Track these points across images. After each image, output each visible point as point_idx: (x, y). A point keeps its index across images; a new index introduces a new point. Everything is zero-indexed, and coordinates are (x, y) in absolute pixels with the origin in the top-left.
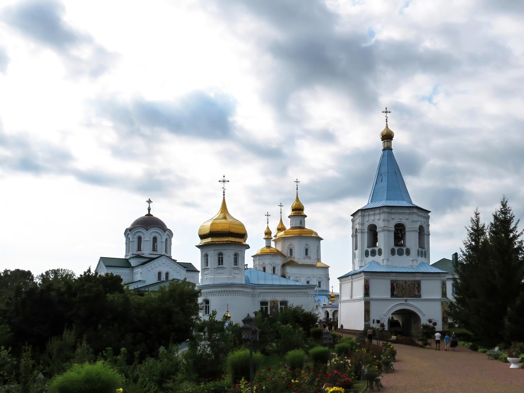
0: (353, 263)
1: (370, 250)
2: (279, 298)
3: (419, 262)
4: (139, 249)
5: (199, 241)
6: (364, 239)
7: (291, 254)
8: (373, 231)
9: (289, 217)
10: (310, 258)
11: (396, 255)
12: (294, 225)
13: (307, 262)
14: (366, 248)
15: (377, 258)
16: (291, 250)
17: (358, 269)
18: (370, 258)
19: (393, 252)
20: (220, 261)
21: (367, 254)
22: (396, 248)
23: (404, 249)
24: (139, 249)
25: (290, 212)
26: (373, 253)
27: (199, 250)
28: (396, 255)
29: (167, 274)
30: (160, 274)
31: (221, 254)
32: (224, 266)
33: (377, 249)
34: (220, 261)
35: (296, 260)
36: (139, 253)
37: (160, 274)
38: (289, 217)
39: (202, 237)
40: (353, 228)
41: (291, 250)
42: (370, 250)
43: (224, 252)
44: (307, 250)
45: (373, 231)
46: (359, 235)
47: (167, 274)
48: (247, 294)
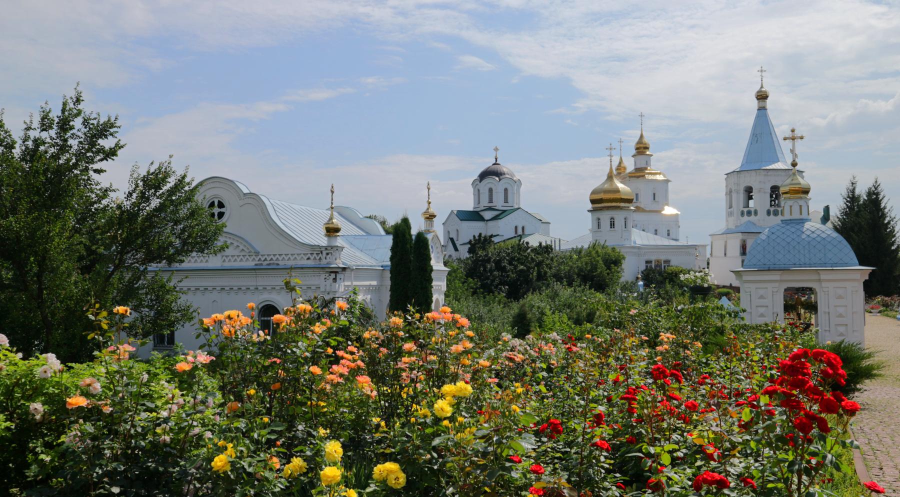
0: (727, 221)
1: (746, 210)
2: (663, 258)
4: (491, 201)
5: (590, 206)
8: (749, 191)
11: (772, 216)
12: (638, 166)
13: (654, 207)
15: (753, 218)
16: (637, 195)
17: (732, 227)
18: (746, 218)
19: (769, 213)
20: (612, 225)
21: (742, 214)
22: (772, 209)
23: (780, 209)
24: (491, 201)
25: (634, 152)
26: (749, 213)
27: (590, 214)
28: (772, 216)
29: (523, 228)
30: (516, 227)
33: (753, 210)
34: (612, 225)
35: (642, 206)
36: (490, 205)
37: (516, 227)
39: (593, 201)
41: (637, 195)
42: (746, 210)
43: (616, 217)
45: (749, 191)
46: (734, 195)
47: (523, 228)
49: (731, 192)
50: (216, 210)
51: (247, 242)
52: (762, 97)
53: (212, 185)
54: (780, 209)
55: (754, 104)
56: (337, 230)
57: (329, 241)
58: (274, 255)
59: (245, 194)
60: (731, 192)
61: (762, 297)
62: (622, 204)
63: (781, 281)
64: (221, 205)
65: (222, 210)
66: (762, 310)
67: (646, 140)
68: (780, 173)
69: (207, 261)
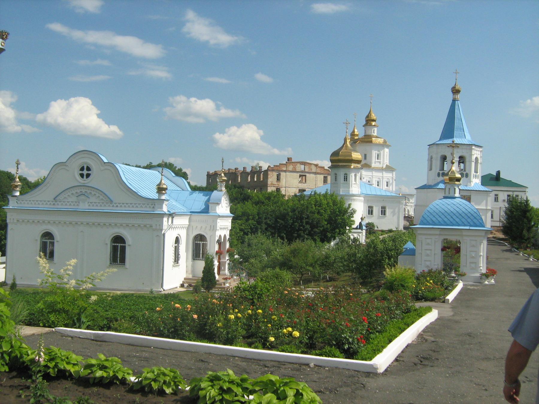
1: (441, 172)
3: (474, 182)
6: (437, 163)
7: (365, 158)
9: (363, 126)
10: (380, 162)
12: (367, 134)
14: (438, 171)
18: (441, 178)
21: (439, 175)
25: (364, 123)
31: (346, 174)
32: (348, 182)
34: (346, 179)
38: (363, 126)
39: (332, 161)
40: (429, 154)
41: (365, 155)
42: (441, 172)
43: (348, 173)
44: (378, 155)
46: (434, 161)
48: (360, 201)
49: (432, 158)
50: (85, 172)
51: (105, 194)
52: (455, 91)
53: (83, 156)
54: (465, 173)
55: (450, 96)
56: (165, 189)
57: (159, 196)
58: (123, 204)
59: (105, 163)
60: (432, 158)
61: (428, 244)
62: (353, 166)
63: (440, 234)
64: (88, 169)
65: (89, 172)
66: (428, 252)
67: (373, 116)
68: (465, 147)
69: (78, 205)
